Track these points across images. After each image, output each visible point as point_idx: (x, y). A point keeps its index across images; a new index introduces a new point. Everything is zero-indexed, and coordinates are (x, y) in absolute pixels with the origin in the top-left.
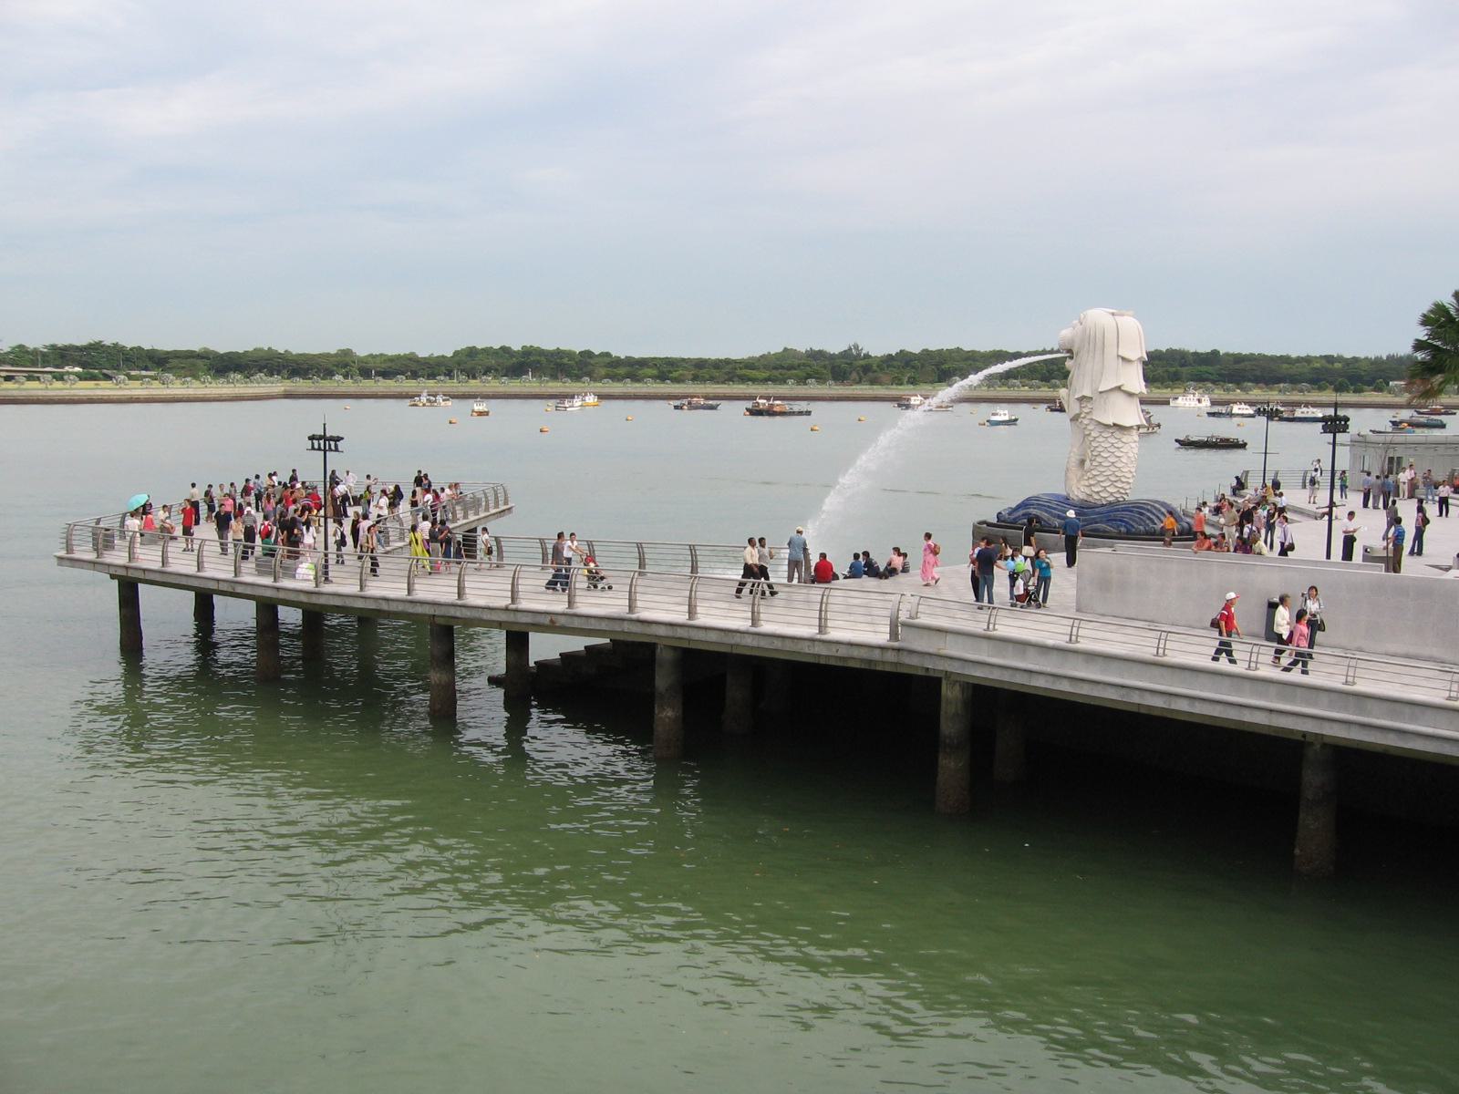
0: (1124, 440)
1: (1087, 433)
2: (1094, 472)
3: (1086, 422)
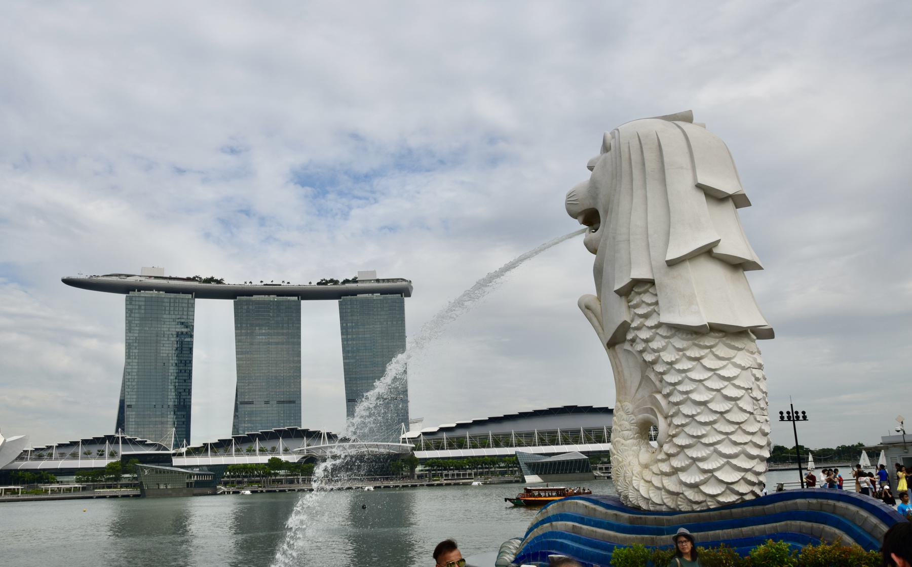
0: (737, 360)
1: (649, 357)
2: (681, 441)
3: (644, 335)
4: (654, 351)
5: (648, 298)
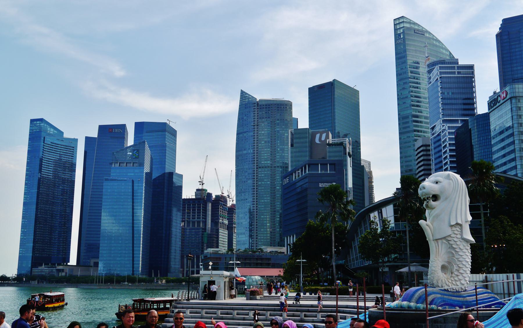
1: (454, 246)
3: (455, 239)
4: (457, 245)
5: (458, 229)
